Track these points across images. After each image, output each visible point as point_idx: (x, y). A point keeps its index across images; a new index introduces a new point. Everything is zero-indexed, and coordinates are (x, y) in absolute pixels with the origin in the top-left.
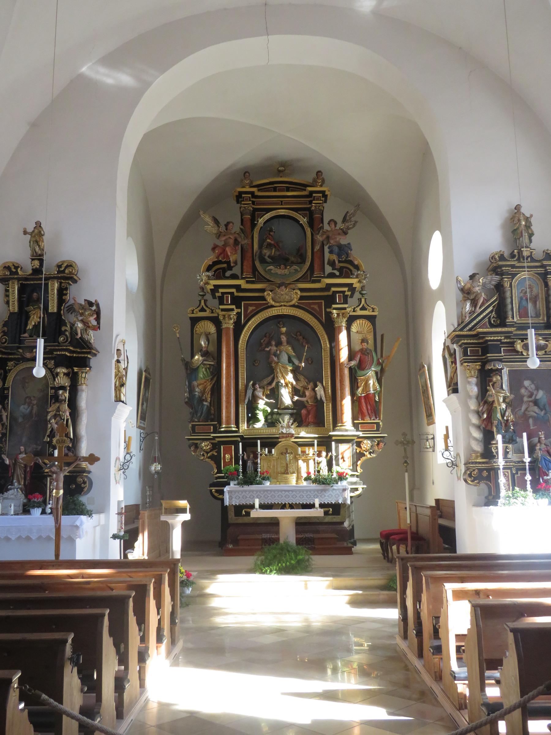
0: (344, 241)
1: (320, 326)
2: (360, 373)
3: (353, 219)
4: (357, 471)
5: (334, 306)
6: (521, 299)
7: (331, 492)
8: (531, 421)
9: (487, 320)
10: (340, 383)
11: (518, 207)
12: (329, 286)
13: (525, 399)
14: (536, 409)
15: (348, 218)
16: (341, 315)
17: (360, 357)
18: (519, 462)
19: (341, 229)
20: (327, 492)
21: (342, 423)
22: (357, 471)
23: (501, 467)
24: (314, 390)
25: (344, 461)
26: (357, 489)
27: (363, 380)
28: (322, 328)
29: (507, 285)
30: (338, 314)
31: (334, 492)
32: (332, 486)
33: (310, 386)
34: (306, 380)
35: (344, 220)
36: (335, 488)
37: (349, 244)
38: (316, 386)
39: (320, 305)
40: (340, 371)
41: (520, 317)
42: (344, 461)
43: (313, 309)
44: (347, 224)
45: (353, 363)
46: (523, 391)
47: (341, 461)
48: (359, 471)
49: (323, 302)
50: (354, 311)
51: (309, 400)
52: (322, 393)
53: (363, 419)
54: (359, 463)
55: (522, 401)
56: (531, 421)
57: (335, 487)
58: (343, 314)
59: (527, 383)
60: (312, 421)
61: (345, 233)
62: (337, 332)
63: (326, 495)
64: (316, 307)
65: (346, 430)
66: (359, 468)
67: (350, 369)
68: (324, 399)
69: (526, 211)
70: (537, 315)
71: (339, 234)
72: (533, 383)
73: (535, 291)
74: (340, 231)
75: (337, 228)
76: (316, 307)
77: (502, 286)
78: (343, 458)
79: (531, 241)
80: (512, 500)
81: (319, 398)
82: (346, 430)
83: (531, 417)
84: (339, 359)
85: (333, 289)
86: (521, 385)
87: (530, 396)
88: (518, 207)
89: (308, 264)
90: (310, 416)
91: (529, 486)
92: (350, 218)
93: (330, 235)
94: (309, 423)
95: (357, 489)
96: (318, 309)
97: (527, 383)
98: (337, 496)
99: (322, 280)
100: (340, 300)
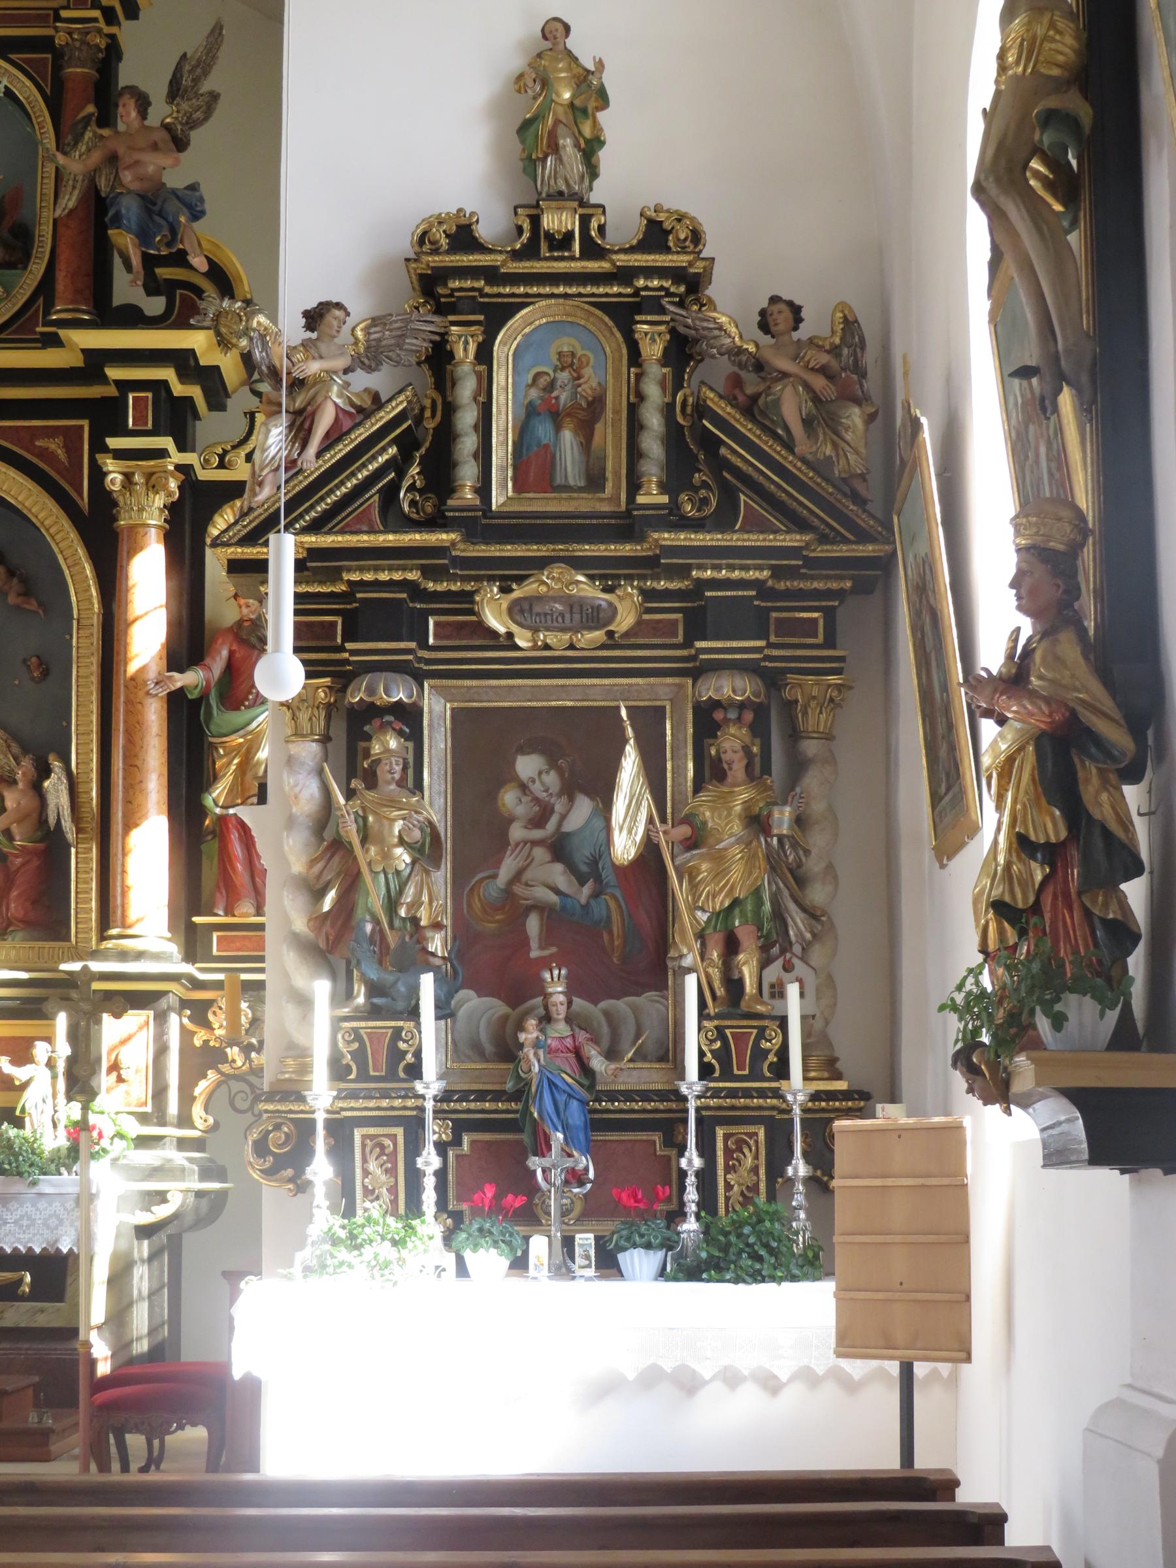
0: (176, 174)
1: (66, 523)
2: (222, 718)
3: (206, 86)
4: (193, 1127)
5: (113, 443)
6: (528, 416)
7: (28, 1208)
8: (533, 924)
9: (373, 497)
10: (126, 757)
11: (555, 31)
12: (97, 360)
13: (517, 832)
14: (558, 874)
15: (186, 81)
16: (137, 478)
17: (231, 654)
18: (662, 1096)
19: (167, 127)
20: (13, 1205)
21: (124, 925)
22: (193, 1127)
23: (320, 1118)
24: (37, 787)
25: (120, 1080)
26: (161, 1197)
27: (232, 752)
28: (73, 535)
29: (465, 350)
30: (128, 477)
31: (42, 1204)
32: (34, 1183)
33: (24, 771)
34: (16, 749)
35: (175, 91)
36: (47, 1190)
37: (193, 187)
38: (44, 771)
39: (71, 438)
40: (128, 712)
41: (520, 485)
42: (120, 1080)
43: (44, 454)
44: (185, 106)
45: (190, 679)
46: (509, 798)
47: (105, 1080)
48: (198, 1123)
49: (85, 423)
50: (222, 465)
51: (15, 828)
52: (64, 800)
53: (229, 912)
54: (202, 1088)
55: (500, 843)
56: (533, 924)
57: (48, 1184)
58: (149, 476)
59: (527, 766)
60: (20, 914)
61: (180, 144)
62: (124, 547)
63: (10, 1218)
64: (55, 446)
65: (139, 955)
66: (197, 1111)
67: (177, 702)
68: (67, 825)
69: (584, 46)
70: (595, 481)
71: (155, 147)
72: (553, 764)
73: (591, 379)
74: (164, 135)
75: (153, 120)
76: (55, 446)
77: (451, 355)
78: (115, 1067)
79: (593, 172)
80: (343, 1254)
81: (52, 821)
82: (139, 955)
83: (539, 907)
84: (126, 664)
85: (115, 373)
86: (506, 776)
87: (538, 821)
88: (555, 31)
89: (37, 269)
90: (14, 893)
91: (429, 1197)
92: (196, 81)
93: (121, 151)
94: (10, 924)
95: (161, 1197)
96: (61, 453)
97: (527, 766)
98: (53, 1222)
99: (62, 333)
100: (140, 418)
